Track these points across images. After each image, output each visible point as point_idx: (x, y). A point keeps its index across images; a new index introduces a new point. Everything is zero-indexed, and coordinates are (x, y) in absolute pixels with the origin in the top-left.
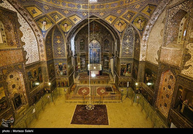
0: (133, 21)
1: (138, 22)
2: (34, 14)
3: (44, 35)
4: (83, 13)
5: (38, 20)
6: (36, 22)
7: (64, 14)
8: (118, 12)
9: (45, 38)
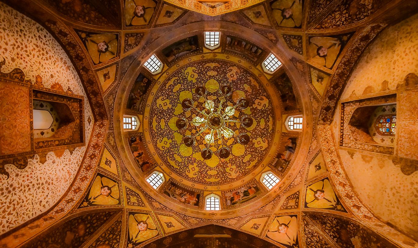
0: (306, 203)
1: (316, 198)
2: (106, 164)
3: (82, 205)
4: (190, 218)
5: (102, 176)
6: (95, 174)
7: (151, 204)
8: (268, 208)
9: (78, 212)
